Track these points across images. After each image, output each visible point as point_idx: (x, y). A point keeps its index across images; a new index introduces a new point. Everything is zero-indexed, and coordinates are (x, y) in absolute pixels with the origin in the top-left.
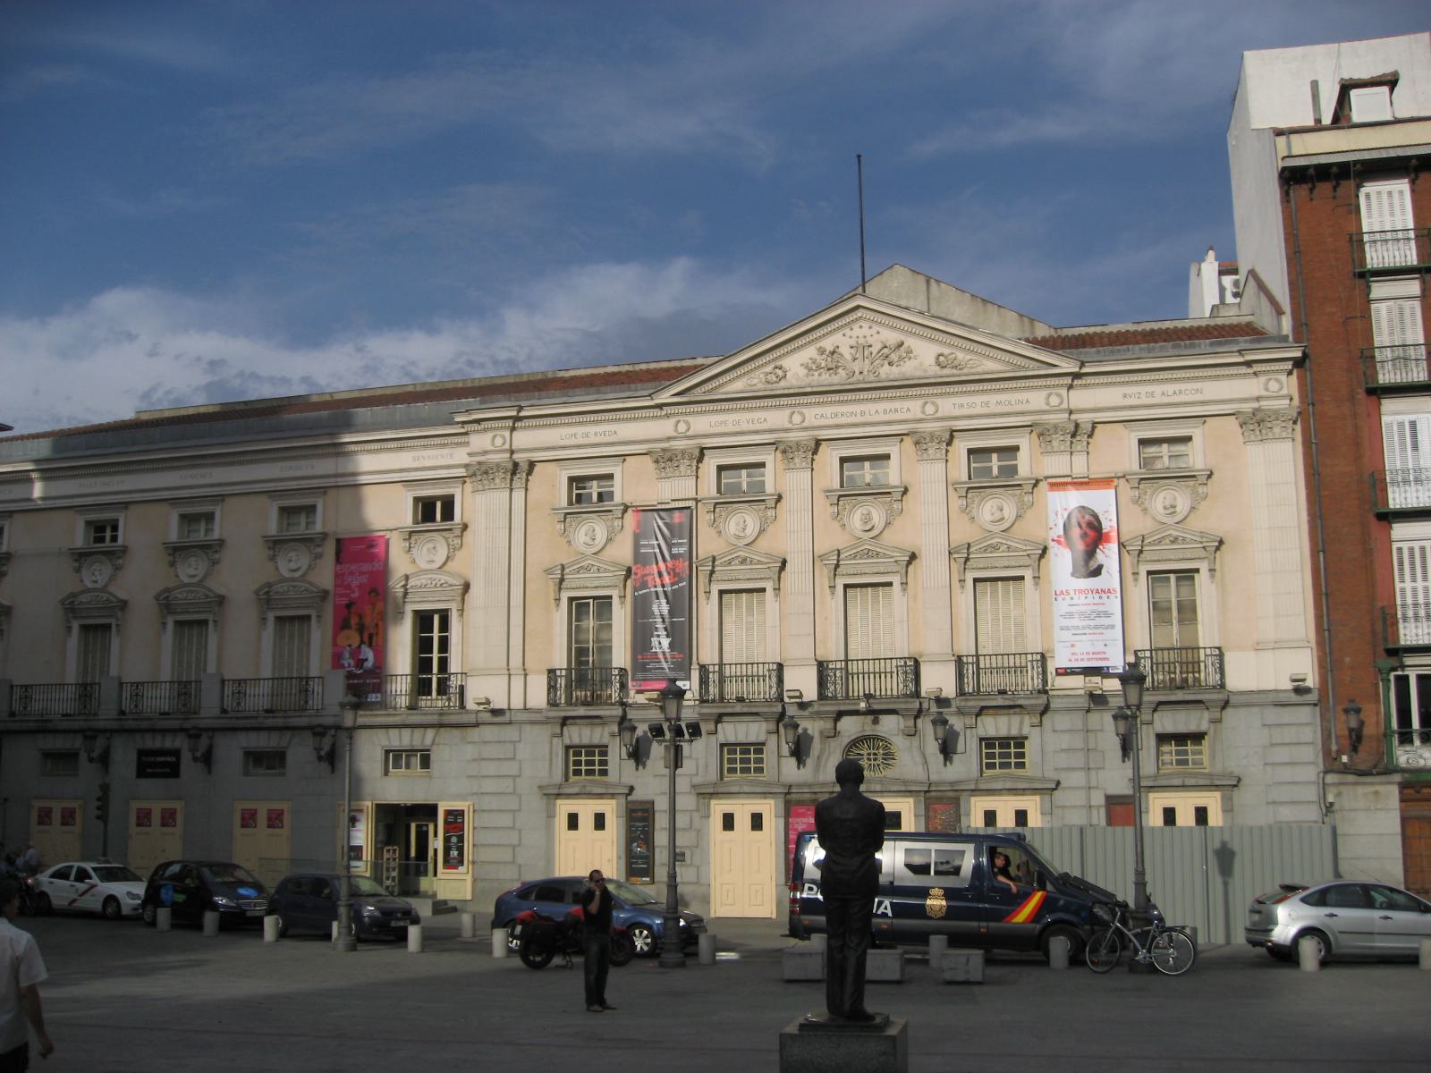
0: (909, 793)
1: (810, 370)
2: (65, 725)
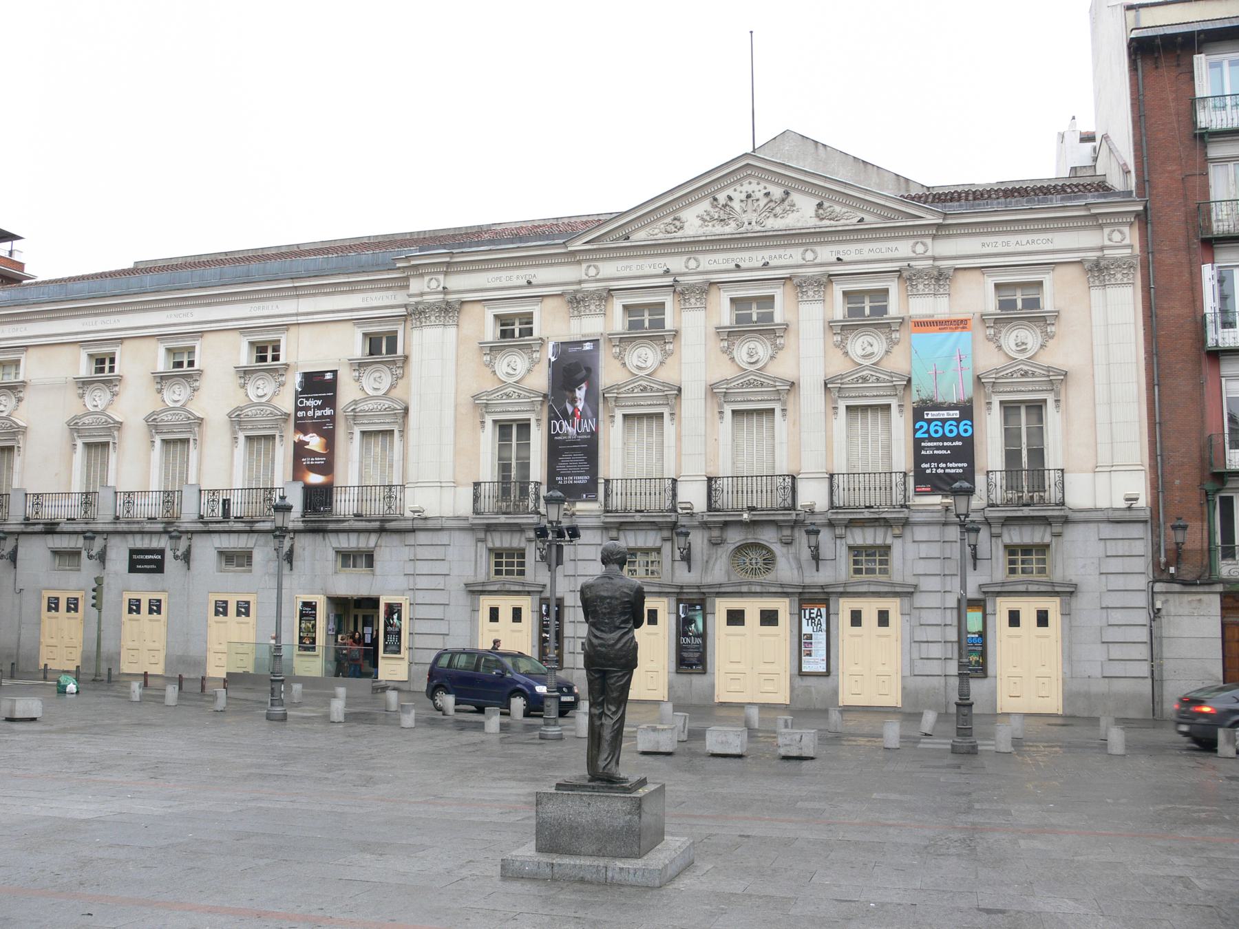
0: (786, 594)
1: (704, 221)
2: (70, 528)
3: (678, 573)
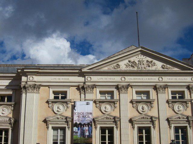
1: (127, 66)
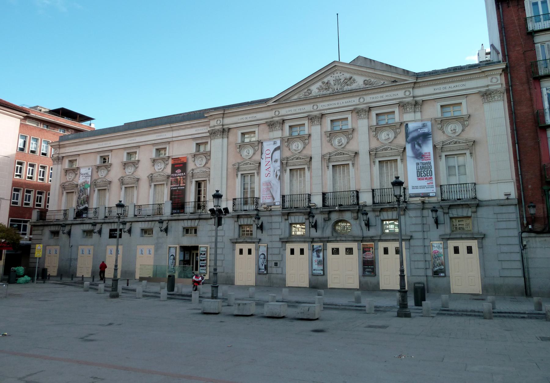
0: (355, 241)
3: (311, 233)
